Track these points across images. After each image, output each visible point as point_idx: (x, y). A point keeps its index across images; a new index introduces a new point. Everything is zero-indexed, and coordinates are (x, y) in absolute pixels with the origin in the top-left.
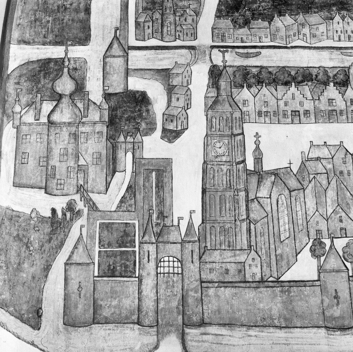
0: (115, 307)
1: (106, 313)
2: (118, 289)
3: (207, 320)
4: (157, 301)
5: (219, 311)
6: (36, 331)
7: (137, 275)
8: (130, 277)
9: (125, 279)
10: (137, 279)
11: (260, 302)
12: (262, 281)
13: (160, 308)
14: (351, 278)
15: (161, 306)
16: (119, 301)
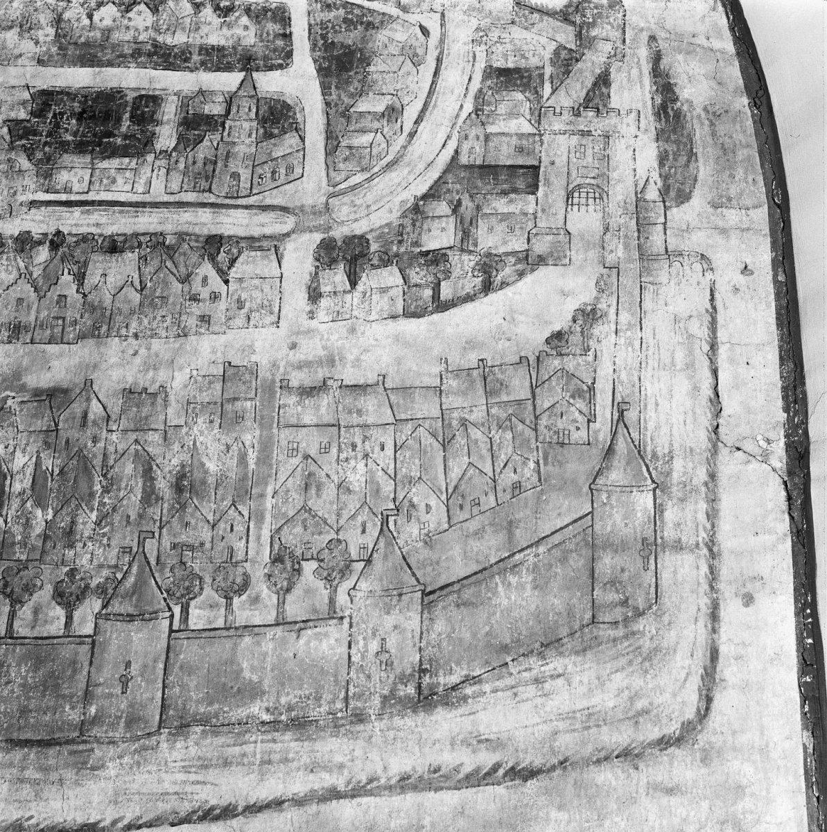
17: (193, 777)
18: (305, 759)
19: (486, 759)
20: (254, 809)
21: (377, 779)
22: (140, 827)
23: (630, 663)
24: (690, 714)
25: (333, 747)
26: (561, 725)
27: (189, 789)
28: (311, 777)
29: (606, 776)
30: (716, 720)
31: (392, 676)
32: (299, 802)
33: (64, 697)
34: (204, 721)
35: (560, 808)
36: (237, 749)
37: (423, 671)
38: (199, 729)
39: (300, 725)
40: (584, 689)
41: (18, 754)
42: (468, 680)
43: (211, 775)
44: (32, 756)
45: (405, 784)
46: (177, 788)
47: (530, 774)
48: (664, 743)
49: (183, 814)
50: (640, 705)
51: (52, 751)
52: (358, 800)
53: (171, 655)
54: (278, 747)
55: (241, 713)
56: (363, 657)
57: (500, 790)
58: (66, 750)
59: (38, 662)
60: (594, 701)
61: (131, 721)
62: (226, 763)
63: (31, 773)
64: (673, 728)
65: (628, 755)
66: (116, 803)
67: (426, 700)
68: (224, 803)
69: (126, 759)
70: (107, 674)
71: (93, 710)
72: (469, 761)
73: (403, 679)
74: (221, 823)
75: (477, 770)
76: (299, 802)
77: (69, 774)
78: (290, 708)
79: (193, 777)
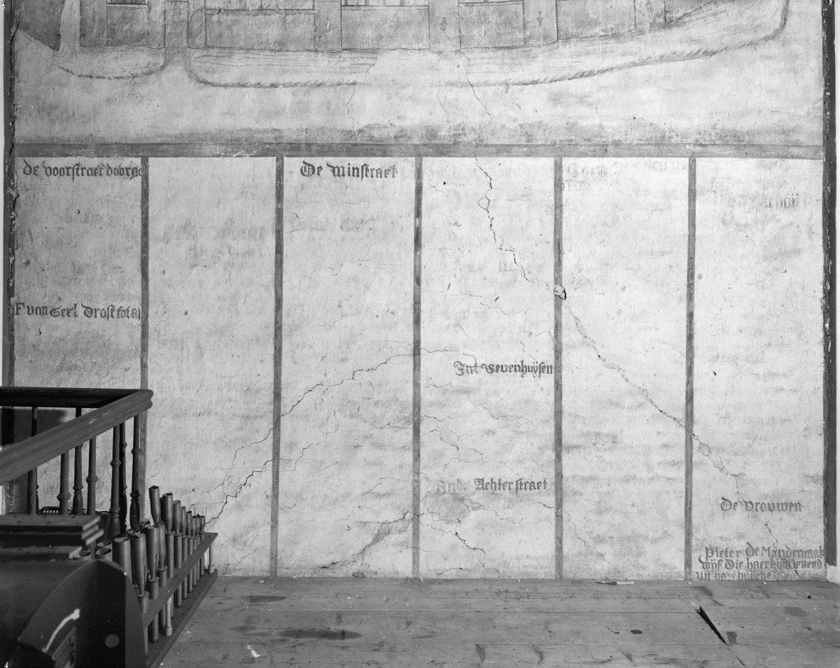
0: (127, 31)
1: (120, 36)
2: (129, 15)
3: (209, 44)
4: (165, 27)
5: (220, 36)
6: (56, 52)
7: (146, 2)
8: (140, 4)
9: (136, 6)
10: (146, 6)
11: (258, 28)
12: (261, 9)
13: (167, 33)
14: (343, 8)
15: (168, 30)
16: (131, 26)
17: (575, 60)
18: (621, 51)
19: (695, 48)
20: (602, 72)
21: (651, 58)
22: (556, 81)
23: (752, 5)
24: (777, 26)
25: (631, 45)
26: (725, 33)
27: (574, 65)
28: (624, 58)
29: (744, 53)
30: (788, 29)
31: (653, 14)
32: (620, 68)
33: (515, 28)
34: (576, 36)
35: (726, 66)
36: (592, 47)
37: (666, 12)
38: (574, 40)
39: (616, 36)
40: (733, 18)
41: (500, 53)
42: (685, 15)
43: (582, 58)
44: (506, 54)
45: (662, 59)
46: (569, 64)
47: (714, 53)
48: (767, 39)
49: (572, 75)
50: (757, 23)
51: (514, 51)
52: (643, 67)
53: (558, 8)
54: (608, 46)
55: (592, 32)
56: (641, 6)
57: (701, 60)
58: (520, 50)
59: (501, 13)
60: (737, 23)
61: (546, 37)
62: (588, 53)
63: (507, 61)
64: (771, 32)
65: (752, 44)
66: (545, 72)
67: (668, 24)
68: (589, 70)
69: (546, 53)
70: (531, 17)
71: (528, 33)
72: (688, 48)
73: (658, 15)
74: (589, 78)
75: (691, 53)
76: (620, 68)
77: (523, 60)
78: (612, 29)
79: (575, 60)
